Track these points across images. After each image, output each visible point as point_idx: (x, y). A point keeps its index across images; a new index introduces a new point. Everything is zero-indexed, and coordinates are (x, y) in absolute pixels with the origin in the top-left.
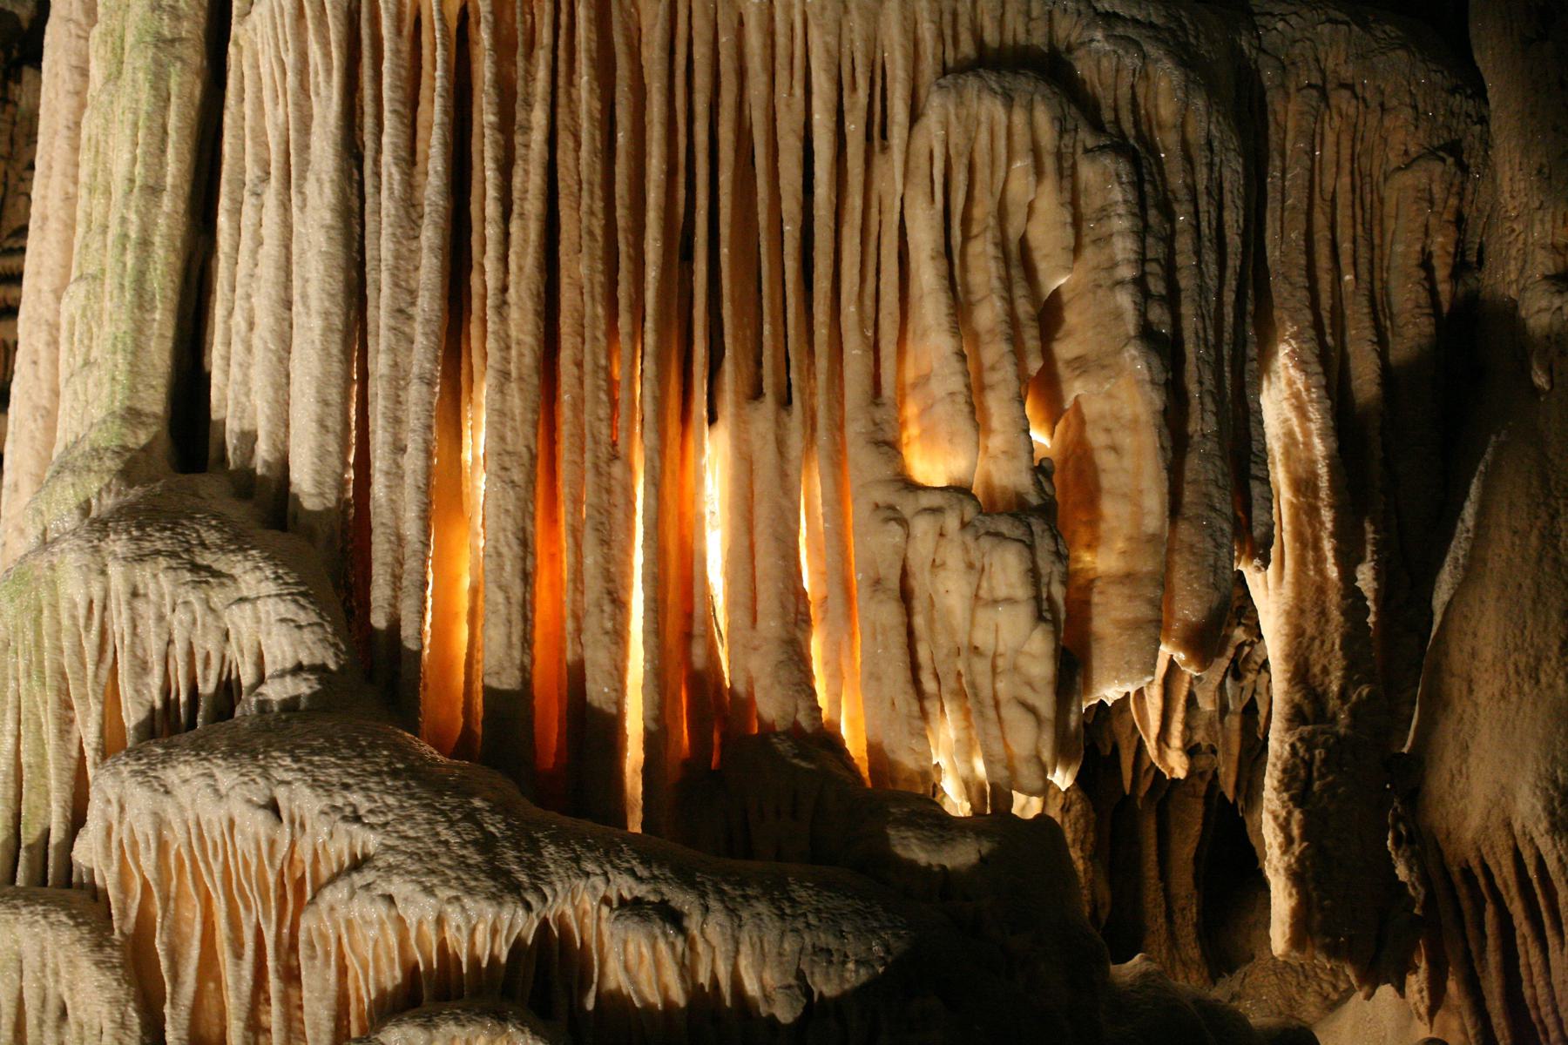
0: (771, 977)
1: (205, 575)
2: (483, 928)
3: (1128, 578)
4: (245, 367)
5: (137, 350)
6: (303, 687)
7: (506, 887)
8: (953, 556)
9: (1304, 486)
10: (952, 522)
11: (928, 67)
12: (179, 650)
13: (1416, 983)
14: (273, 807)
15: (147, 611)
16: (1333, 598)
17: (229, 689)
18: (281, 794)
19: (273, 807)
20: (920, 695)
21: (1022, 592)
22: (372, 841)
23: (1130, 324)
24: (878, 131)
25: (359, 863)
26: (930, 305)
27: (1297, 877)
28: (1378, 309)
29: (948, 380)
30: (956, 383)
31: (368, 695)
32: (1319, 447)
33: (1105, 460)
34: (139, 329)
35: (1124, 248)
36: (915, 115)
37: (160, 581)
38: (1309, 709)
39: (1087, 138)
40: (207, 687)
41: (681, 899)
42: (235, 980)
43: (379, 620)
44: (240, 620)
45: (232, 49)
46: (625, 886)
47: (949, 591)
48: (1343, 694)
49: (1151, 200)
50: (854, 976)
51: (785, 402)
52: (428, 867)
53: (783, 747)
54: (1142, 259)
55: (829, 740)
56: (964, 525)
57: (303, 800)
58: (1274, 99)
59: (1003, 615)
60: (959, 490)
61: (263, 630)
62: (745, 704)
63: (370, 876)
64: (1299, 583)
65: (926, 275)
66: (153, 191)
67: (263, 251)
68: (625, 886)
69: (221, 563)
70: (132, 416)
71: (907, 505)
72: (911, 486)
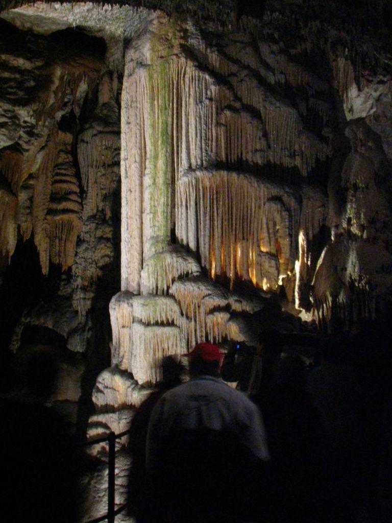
0: (250, 309)
1: (185, 260)
2: (222, 302)
3: (284, 263)
4: (181, 230)
5: (167, 227)
6: (198, 274)
7: (226, 298)
8: (267, 261)
9: (303, 251)
10: (267, 257)
11: (266, 199)
12: (182, 268)
13: (312, 312)
14: (199, 288)
15: (179, 264)
16: (306, 265)
17: (188, 273)
18: (200, 287)
19: (199, 288)
20: (262, 275)
21: (275, 266)
22: (210, 292)
23: (287, 233)
24: (259, 207)
25: (209, 295)
26: (265, 230)
27: (300, 299)
28: (313, 226)
29: (267, 239)
30: (268, 240)
31: (203, 276)
32: (305, 246)
33: (283, 249)
34: (167, 223)
35: (287, 224)
36: (264, 205)
37: (180, 260)
38: (301, 279)
39: (284, 209)
40: (185, 273)
41: (241, 299)
42: (192, 307)
43: (203, 265)
44: (190, 265)
45: (176, 186)
46: (236, 298)
47: (266, 265)
48: (306, 278)
49: (290, 216)
50: (259, 309)
51: (247, 240)
52: (218, 296)
53: (248, 282)
54: (289, 225)
55: (251, 282)
56: (269, 258)
57: (203, 288)
58: (304, 200)
59: (272, 268)
60: (267, 253)
61: (192, 267)
62: (241, 277)
63: (211, 296)
64: (302, 262)
65: (265, 226)
66: (167, 205)
67: (183, 215)
68: (236, 298)
69: (188, 258)
70: (167, 236)
71: (262, 254)
72: (262, 252)
